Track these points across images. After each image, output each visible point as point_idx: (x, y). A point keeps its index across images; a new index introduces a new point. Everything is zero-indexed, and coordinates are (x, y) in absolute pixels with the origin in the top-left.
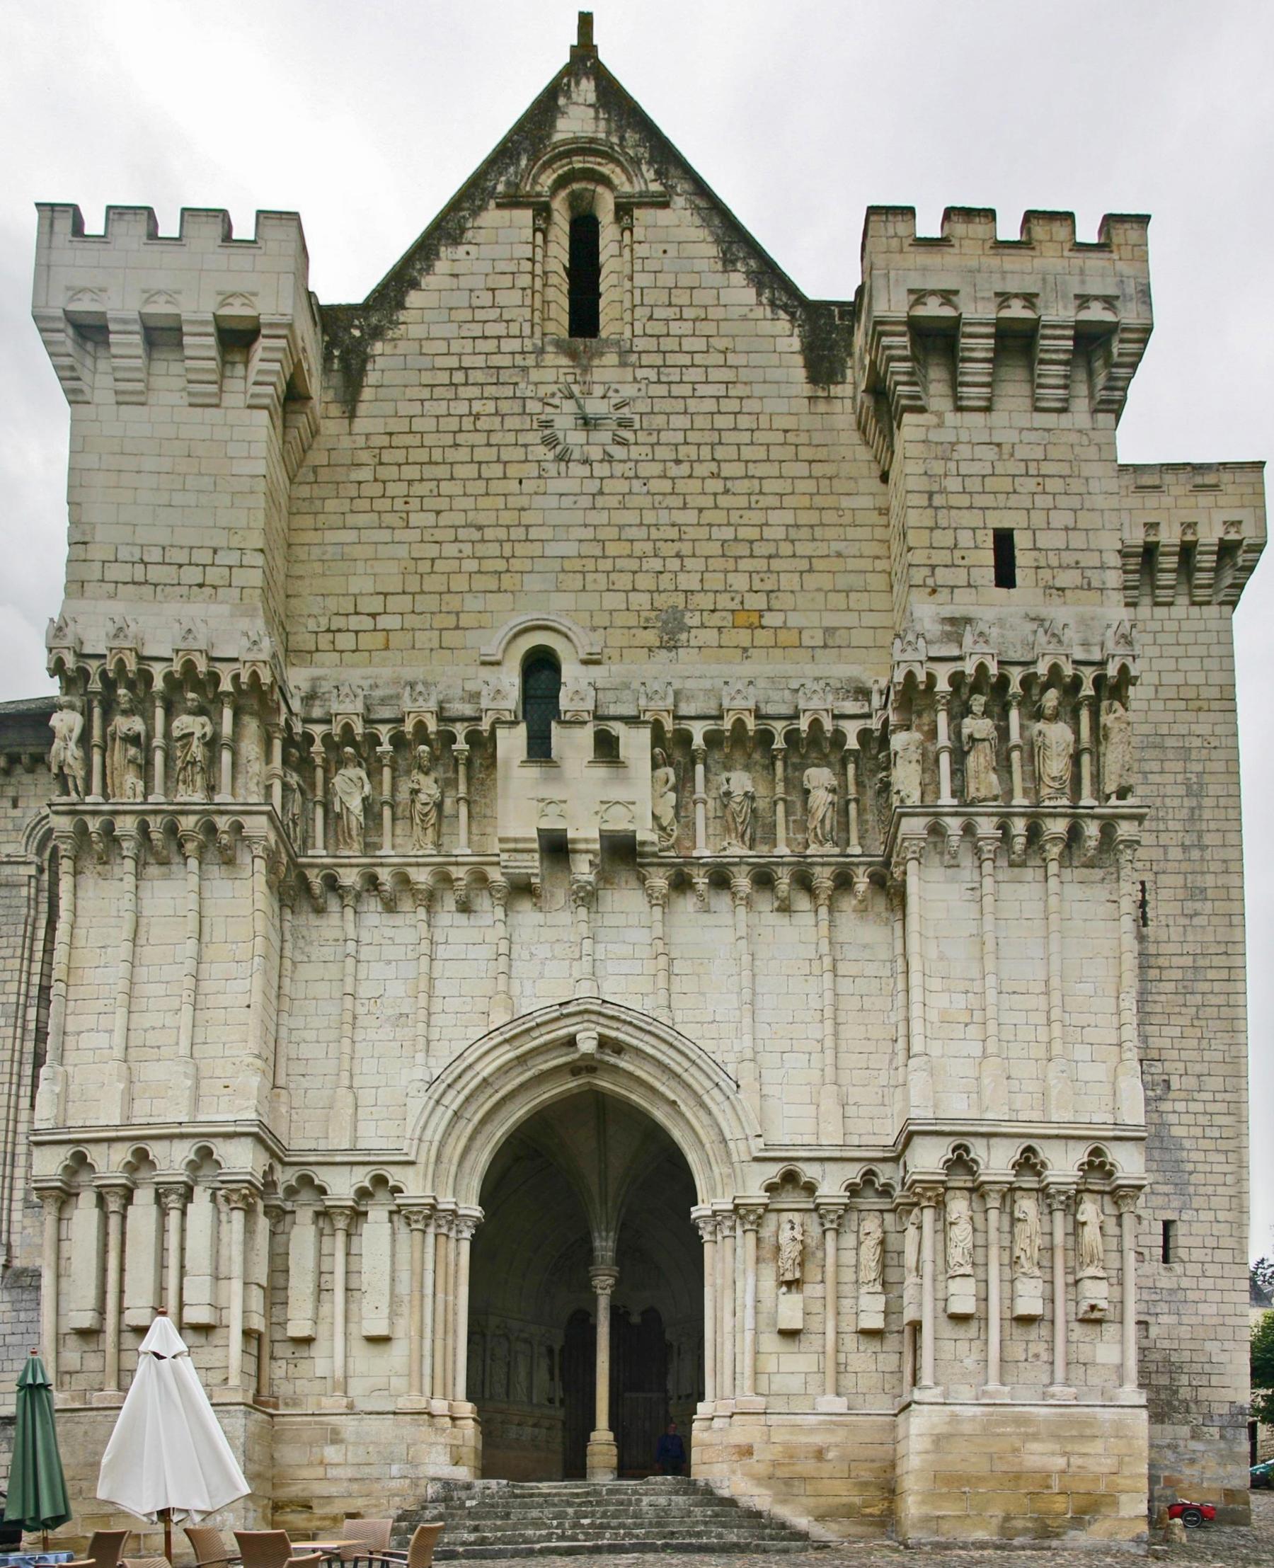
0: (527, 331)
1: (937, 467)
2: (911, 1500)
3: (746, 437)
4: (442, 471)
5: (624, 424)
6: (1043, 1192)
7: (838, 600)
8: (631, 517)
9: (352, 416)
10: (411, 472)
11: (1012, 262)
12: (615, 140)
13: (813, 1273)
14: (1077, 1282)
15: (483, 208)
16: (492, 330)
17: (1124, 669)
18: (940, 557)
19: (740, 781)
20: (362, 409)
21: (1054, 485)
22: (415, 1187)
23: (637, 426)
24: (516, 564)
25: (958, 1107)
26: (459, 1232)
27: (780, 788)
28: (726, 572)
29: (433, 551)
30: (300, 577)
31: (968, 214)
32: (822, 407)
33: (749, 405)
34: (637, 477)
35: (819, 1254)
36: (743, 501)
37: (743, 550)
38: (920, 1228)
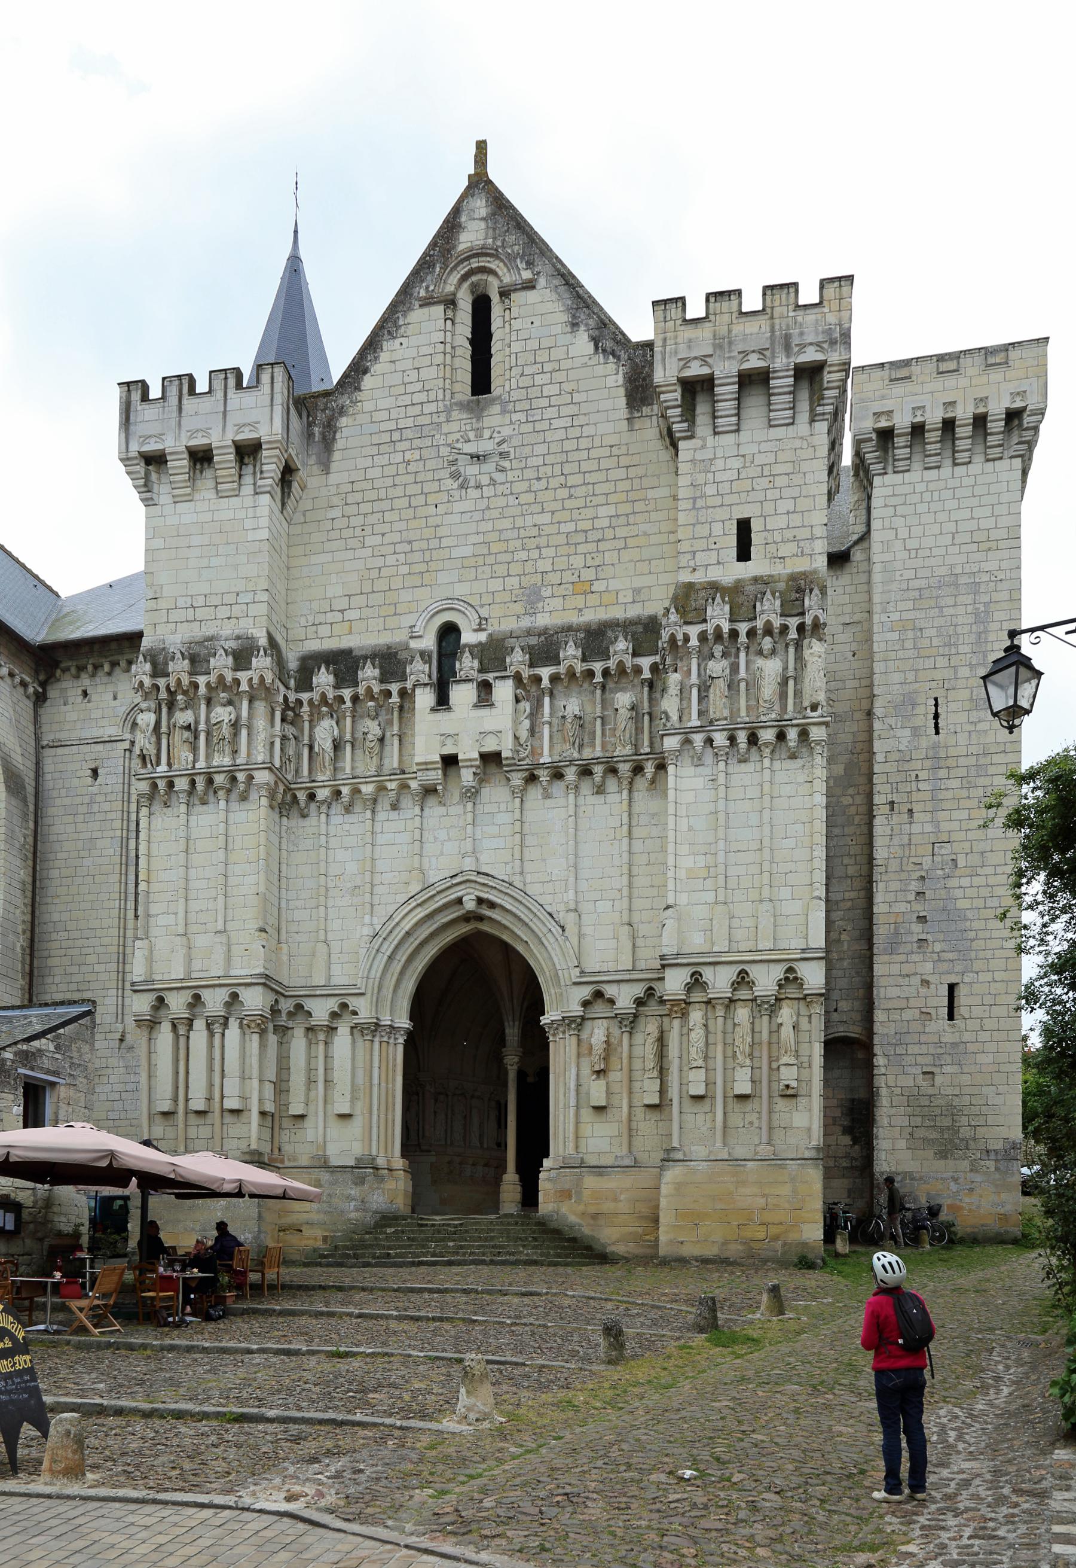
0: (440, 397)
1: (700, 479)
4: (386, 505)
5: (503, 455)
7: (644, 567)
8: (506, 523)
10: (366, 508)
16: (417, 398)
20: (334, 466)
21: (780, 481)
22: (365, 1010)
23: (512, 456)
24: (433, 566)
28: (569, 555)
29: (379, 561)
33: (587, 431)
34: (512, 494)
36: (580, 503)
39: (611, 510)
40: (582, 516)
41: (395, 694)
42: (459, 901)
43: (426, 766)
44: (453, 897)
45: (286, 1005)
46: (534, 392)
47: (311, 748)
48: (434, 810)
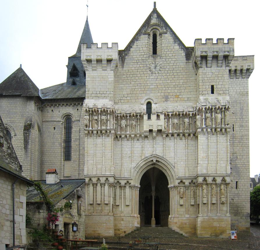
0: (147, 54)
2: (198, 231)
3: (177, 69)
4: (136, 76)
5: (161, 68)
6: (216, 184)
7: (189, 93)
8: (161, 82)
9: (123, 67)
10: (131, 76)
11: (215, 46)
12: (159, 23)
13: (185, 196)
14: (221, 198)
15: (141, 35)
16: (142, 54)
17: (228, 107)
18: (204, 90)
19: (176, 121)
20: (124, 66)
23: (162, 68)
24: (146, 89)
25: (204, 172)
26: (137, 189)
27: (181, 122)
29: (134, 87)
30: (116, 92)
31: (209, 39)
32: (188, 64)
33: (178, 64)
34: (162, 76)
35: (185, 193)
36: (176, 79)
37: (177, 86)
38: (199, 190)
39: (183, 81)
40: (177, 82)
41: (138, 116)
43: (146, 132)
44: (151, 160)
45: (116, 181)
46: (167, 55)
47: (120, 126)
48: (146, 141)
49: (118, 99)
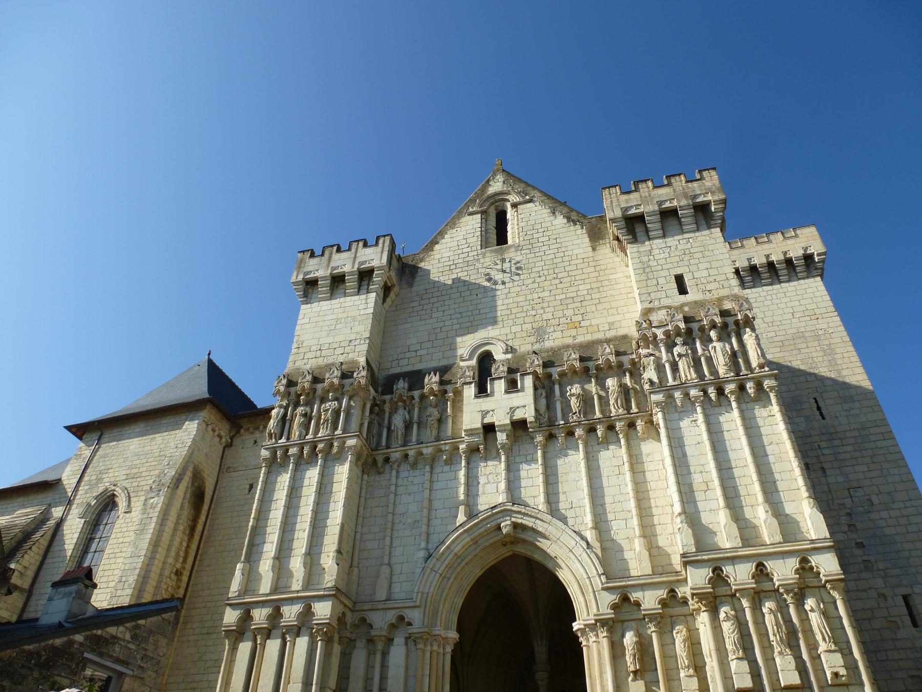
8: (521, 299)
16: (464, 251)
28: (563, 310)
42: (499, 528)
43: (470, 432)
49: (390, 359)
